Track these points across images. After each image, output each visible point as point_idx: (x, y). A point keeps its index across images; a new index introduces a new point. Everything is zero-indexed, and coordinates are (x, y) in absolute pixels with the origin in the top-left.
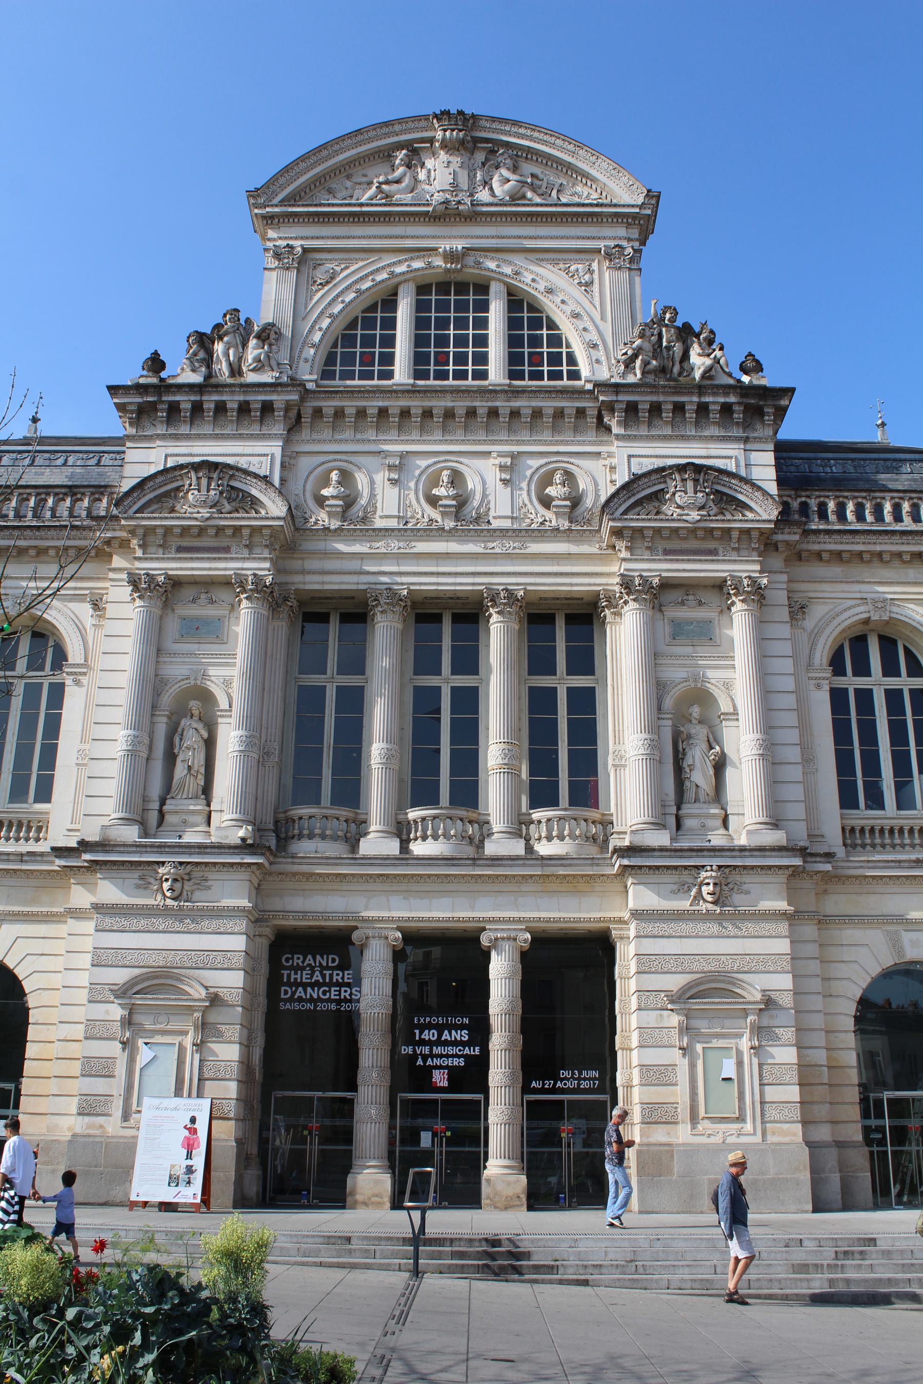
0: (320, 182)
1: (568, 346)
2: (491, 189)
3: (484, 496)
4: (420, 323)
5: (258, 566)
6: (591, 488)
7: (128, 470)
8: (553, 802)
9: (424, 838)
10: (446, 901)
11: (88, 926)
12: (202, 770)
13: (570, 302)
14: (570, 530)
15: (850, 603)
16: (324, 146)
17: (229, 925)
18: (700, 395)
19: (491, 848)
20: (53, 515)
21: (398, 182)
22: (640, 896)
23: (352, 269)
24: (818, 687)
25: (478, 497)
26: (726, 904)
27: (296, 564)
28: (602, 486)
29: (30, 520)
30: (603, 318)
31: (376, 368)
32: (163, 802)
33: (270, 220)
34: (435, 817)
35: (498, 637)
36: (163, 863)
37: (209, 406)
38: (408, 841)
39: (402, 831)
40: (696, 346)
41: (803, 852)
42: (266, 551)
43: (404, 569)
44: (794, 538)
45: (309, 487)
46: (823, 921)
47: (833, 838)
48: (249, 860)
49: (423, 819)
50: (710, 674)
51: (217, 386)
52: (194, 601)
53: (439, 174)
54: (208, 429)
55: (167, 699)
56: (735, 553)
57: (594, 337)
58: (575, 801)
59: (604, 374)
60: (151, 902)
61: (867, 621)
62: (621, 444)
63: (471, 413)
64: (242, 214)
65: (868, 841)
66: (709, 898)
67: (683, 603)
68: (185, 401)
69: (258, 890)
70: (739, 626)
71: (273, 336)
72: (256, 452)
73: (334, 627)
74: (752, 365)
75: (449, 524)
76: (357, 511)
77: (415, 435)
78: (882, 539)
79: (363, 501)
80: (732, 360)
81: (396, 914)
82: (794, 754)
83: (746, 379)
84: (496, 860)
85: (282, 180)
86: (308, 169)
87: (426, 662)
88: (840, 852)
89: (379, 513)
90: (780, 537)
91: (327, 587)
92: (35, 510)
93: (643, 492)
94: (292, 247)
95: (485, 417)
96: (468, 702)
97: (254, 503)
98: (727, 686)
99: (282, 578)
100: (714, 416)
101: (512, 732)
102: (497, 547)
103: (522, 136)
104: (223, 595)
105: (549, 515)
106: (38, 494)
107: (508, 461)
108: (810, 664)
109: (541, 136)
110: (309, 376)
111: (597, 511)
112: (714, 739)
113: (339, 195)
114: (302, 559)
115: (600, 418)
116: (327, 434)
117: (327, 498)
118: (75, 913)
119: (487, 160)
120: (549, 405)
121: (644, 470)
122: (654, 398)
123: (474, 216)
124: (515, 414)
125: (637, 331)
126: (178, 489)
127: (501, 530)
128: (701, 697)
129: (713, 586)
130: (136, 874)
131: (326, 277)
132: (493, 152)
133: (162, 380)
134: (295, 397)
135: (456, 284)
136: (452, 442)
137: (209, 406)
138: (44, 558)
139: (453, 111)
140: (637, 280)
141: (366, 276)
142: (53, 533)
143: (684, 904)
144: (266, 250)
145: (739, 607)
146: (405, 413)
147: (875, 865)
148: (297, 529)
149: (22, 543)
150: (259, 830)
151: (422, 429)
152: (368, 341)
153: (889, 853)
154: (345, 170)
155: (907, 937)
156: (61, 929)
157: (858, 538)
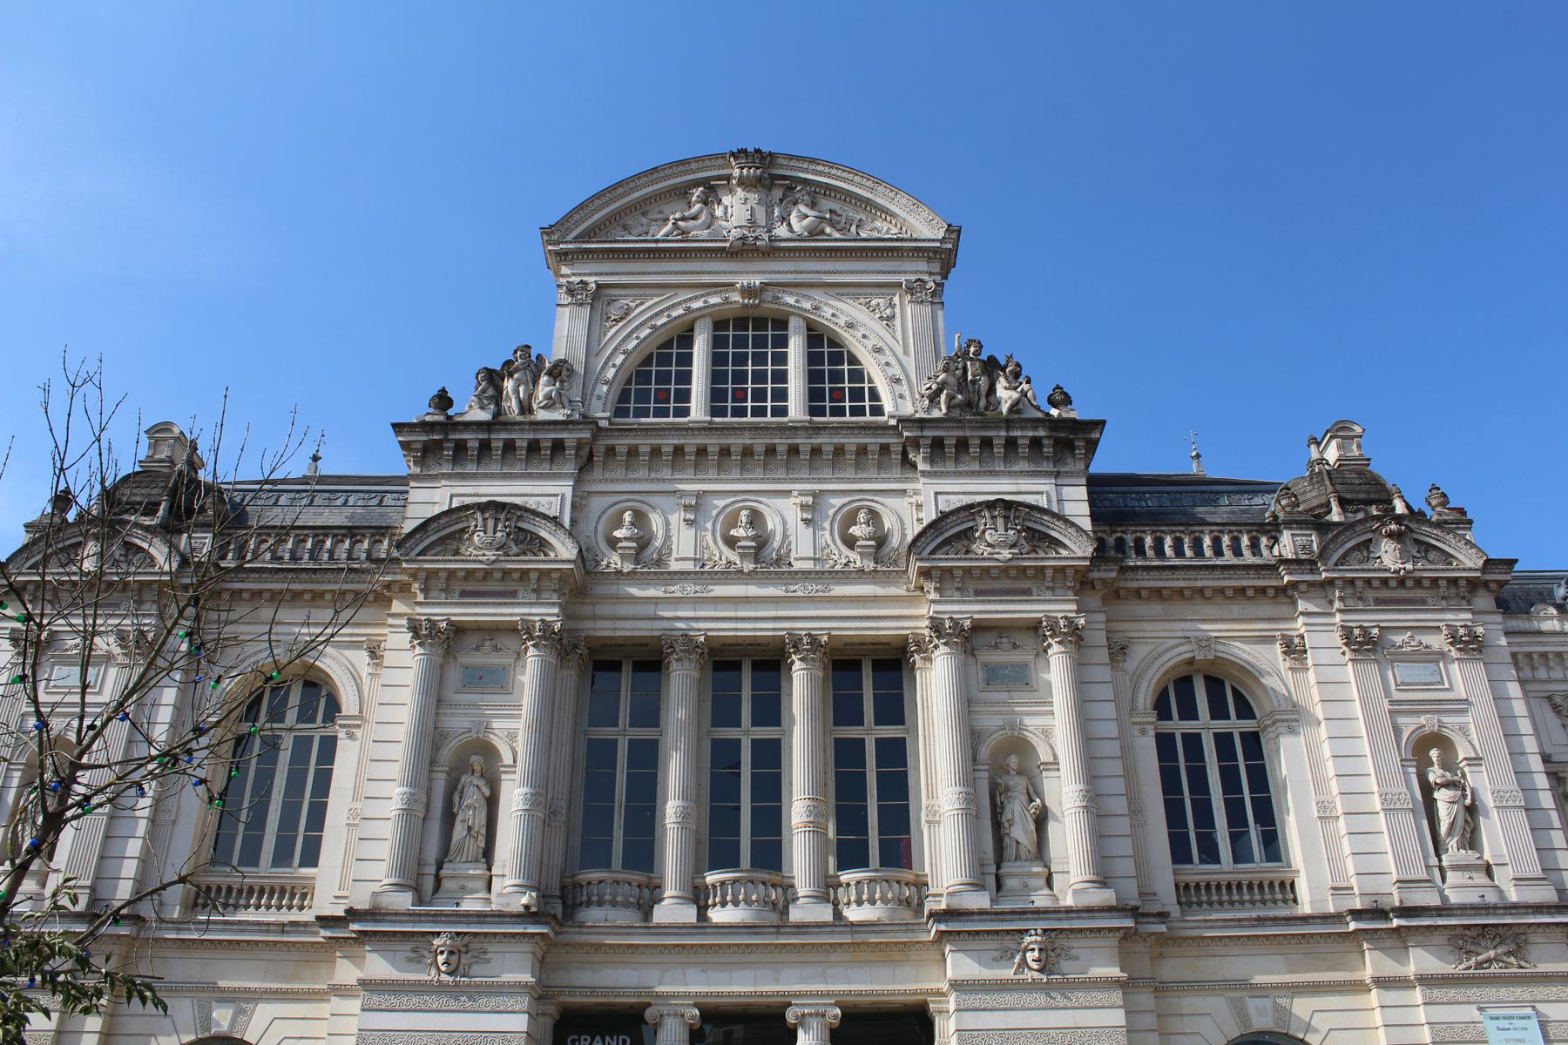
0: (614, 219)
1: (870, 381)
2: (789, 224)
3: (785, 536)
4: (717, 359)
5: (546, 612)
6: (897, 527)
7: (412, 511)
8: (861, 862)
9: (724, 904)
10: (748, 974)
11: (354, 1005)
12: (483, 831)
13: (871, 336)
14: (875, 571)
15: (1172, 642)
16: (620, 184)
17: (509, 1002)
18: (1008, 429)
19: (796, 915)
20: (331, 558)
21: (694, 218)
22: (960, 964)
23: (647, 304)
24: (1143, 732)
25: (778, 538)
26: (1054, 973)
27: (587, 610)
28: (908, 525)
29: (306, 563)
30: (906, 352)
31: (672, 405)
32: (440, 866)
33: (563, 256)
34: (735, 881)
35: (801, 685)
36: (438, 934)
37: (497, 444)
38: (707, 907)
39: (699, 897)
40: (1002, 379)
41: (1134, 912)
42: (555, 596)
43: (700, 614)
44: (1110, 576)
45: (601, 528)
46: (1161, 988)
47: (1167, 897)
48: (532, 930)
49: (723, 883)
50: (1028, 721)
51: (506, 424)
52: (477, 648)
53: (736, 210)
54: (495, 468)
55: (447, 754)
56: (1049, 593)
57: (896, 371)
58: (885, 862)
59: (908, 409)
60: (424, 977)
61: (1191, 661)
62: (927, 481)
63: (771, 451)
64: (535, 251)
65: (1204, 898)
66: (1035, 965)
67: (996, 646)
68: (472, 439)
69: (542, 964)
70: (1056, 669)
71: (565, 373)
72: (548, 493)
73: (626, 676)
74: (1061, 398)
75: (748, 566)
76: (651, 553)
77: (712, 474)
78: (1203, 574)
79: (658, 543)
80: (1039, 393)
81: (693, 989)
82: (1120, 805)
83: (1054, 412)
84: (802, 928)
85: (577, 217)
86: (603, 206)
87: (725, 713)
88: (1175, 911)
89: (674, 555)
90: (1096, 575)
91: (619, 633)
92: (312, 552)
93: (950, 531)
94: (586, 283)
95: (785, 454)
96: (771, 756)
97: (543, 545)
98: (1047, 733)
99: (571, 625)
100: (1023, 451)
101: (817, 787)
102: (799, 590)
103: (821, 174)
104: (510, 642)
105: (853, 555)
106: (315, 536)
107: (810, 500)
108: (1133, 708)
109: (839, 173)
110: (601, 414)
111: (904, 550)
112: (1033, 792)
113: (635, 232)
114: (593, 604)
115: (905, 454)
116: (620, 473)
117: (620, 540)
118: (340, 991)
119: (785, 196)
120: (851, 441)
121: (952, 507)
122: (960, 433)
123: (773, 251)
124: (816, 451)
125: (941, 365)
126: (463, 531)
127: (803, 572)
128: (1019, 746)
129: (1028, 628)
130: (408, 946)
131: (620, 313)
132: (790, 189)
133: (449, 418)
134: (587, 435)
135: (754, 319)
136: (750, 481)
137: (497, 444)
138: (318, 602)
139: (751, 149)
140: (940, 313)
141: (662, 311)
142: (330, 576)
143: (1008, 973)
144: (559, 286)
145: (1055, 649)
146: (702, 451)
147: (1212, 925)
148: (588, 573)
149: (297, 587)
150: (544, 897)
151: (720, 467)
152: (664, 378)
153: (1226, 911)
154: (642, 207)
155: (1252, 1004)
156: (324, 1009)
157: (1178, 575)
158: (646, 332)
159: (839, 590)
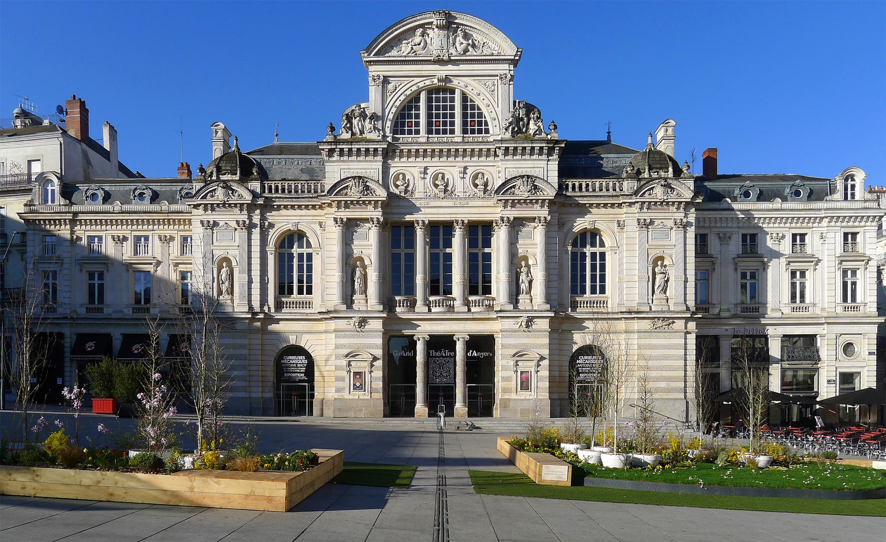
39: (428, 304)
57: (494, 115)
102: (458, 203)
115: (495, 152)
158: (402, 98)
159: (471, 204)
